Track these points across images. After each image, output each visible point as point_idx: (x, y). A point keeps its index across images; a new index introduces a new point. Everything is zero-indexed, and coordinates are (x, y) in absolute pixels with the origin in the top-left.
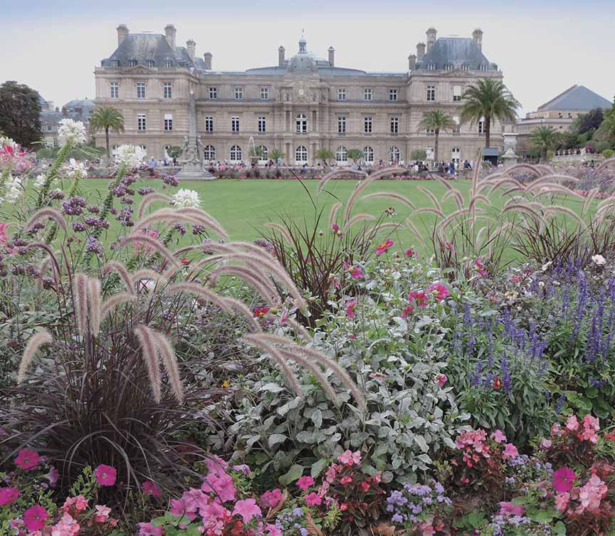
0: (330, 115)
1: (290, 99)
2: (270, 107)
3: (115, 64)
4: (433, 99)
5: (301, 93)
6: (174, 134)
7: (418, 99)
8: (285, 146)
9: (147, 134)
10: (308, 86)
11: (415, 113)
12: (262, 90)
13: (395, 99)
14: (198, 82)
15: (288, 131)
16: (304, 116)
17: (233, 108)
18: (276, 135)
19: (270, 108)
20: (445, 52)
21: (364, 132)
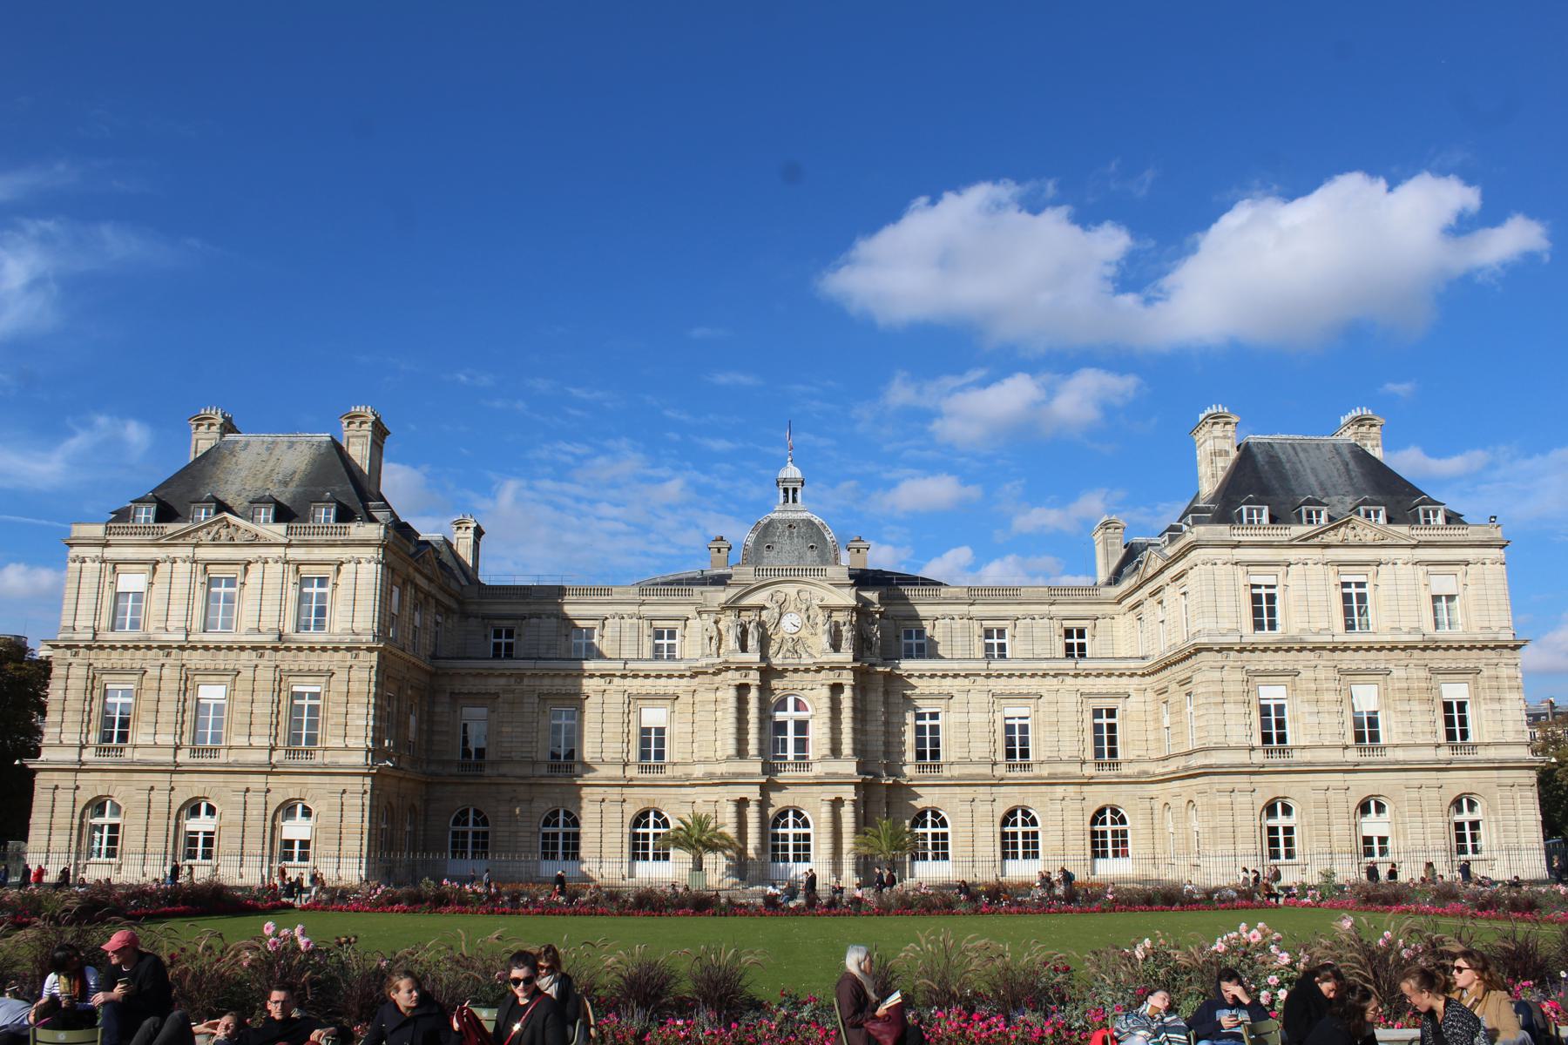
0: (886, 703)
1: (752, 643)
2: (681, 676)
3: (146, 514)
4: (1272, 626)
5: (790, 623)
6: (319, 758)
7: (1226, 624)
8: (730, 809)
9: (223, 757)
10: (816, 602)
11: (1217, 675)
12: (659, 634)
13: (1082, 656)
14: (455, 606)
15: (741, 752)
16: (799, 706)
17: (558, 681)
18: (698, 771)
19: (684, 681)
20: (1282, 477)
21: (1001, 756)
